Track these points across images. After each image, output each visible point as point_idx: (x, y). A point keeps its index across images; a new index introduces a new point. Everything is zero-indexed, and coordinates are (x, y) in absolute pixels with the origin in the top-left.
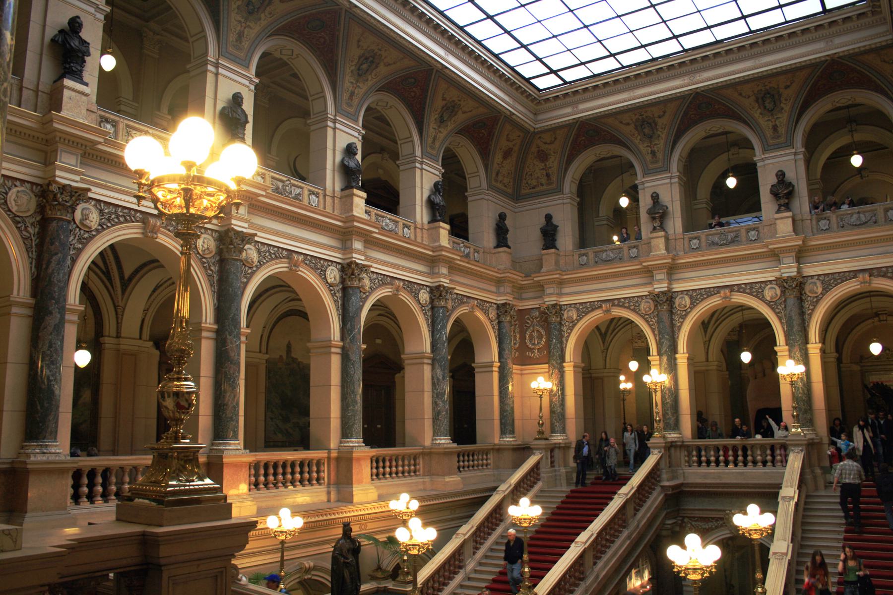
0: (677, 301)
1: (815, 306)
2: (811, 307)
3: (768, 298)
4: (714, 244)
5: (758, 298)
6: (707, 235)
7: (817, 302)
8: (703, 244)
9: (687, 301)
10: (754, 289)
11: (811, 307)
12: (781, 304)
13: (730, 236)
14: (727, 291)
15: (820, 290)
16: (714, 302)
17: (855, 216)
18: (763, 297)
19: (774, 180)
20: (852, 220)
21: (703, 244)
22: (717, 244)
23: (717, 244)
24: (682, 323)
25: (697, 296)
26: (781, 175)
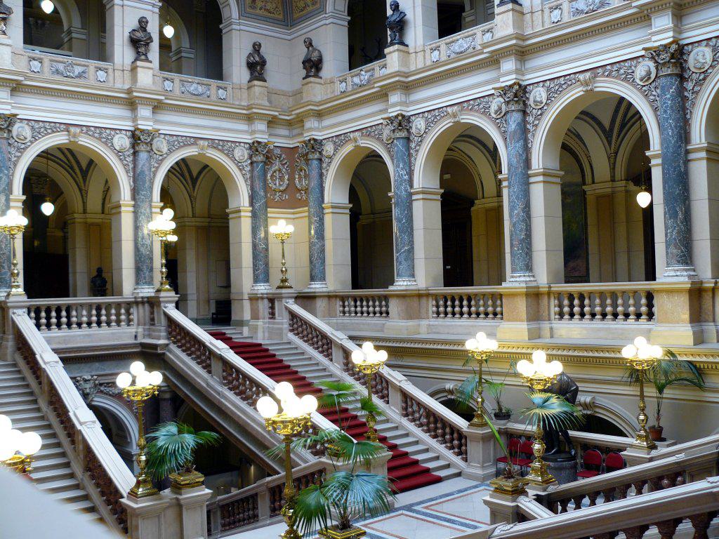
0: (16, 129)
1: (160, 164)
2: (156, 165)
3: (118, 148)
4: (58, 72)
5: (107, 145)
6: (51, 61)
7: (162, 160)
8: (46, 69)
9: (27, 132)
10: (103, 134)
11: (156, 165)
12: (128, 156)
13: (78, 70)
14: (78, 130)
15: (165, 150)
16: (59, 139)
17: (195, 85)
18: (112, 145)
19: (134, 24)
20: (192, 88)
21: (46, 69)
22: (62, 74)
23: (62, 74)
24: (19, 157)
25: (41, 127)
26: (143, 23)
